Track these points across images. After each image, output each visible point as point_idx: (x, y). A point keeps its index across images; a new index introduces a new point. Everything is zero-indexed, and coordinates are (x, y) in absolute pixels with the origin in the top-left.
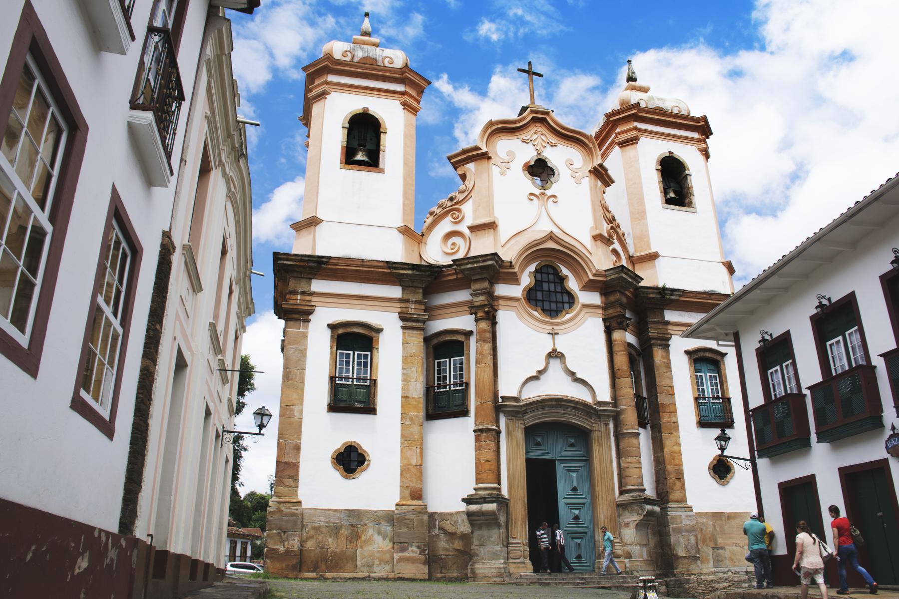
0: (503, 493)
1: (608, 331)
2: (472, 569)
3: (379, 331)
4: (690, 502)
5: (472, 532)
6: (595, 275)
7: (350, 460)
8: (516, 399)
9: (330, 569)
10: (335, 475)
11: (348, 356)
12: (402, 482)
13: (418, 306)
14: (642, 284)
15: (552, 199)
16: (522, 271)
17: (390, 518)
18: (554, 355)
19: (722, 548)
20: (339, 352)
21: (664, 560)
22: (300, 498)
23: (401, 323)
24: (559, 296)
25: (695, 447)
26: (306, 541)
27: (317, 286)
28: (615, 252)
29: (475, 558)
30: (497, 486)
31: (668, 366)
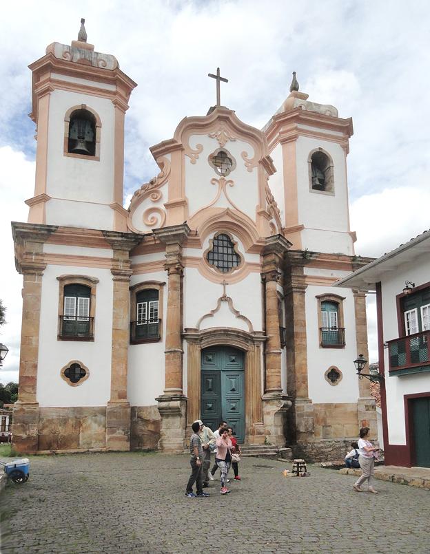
0: (184, 393)
3: (96, 282)
4: (310, 397)
5: (162, 420)
6: (258, 242)
7: (75, 373)
8: (196, 330)
9: (60, 447)
10: (64, 384)
13: (125, 264)
15: (228, 184)
16: (204, 239)
17: (103, 411)
18: (225, 299)
19: (329, 426)
20: (65, 297)
21: (290, 432)
22: (38, 400)
23: (112, 277)
25: (317, 360)
26: (42, 430)
27: (48, 248)
29: (163, 437)
30: (180, 389)
31: (303, 307)
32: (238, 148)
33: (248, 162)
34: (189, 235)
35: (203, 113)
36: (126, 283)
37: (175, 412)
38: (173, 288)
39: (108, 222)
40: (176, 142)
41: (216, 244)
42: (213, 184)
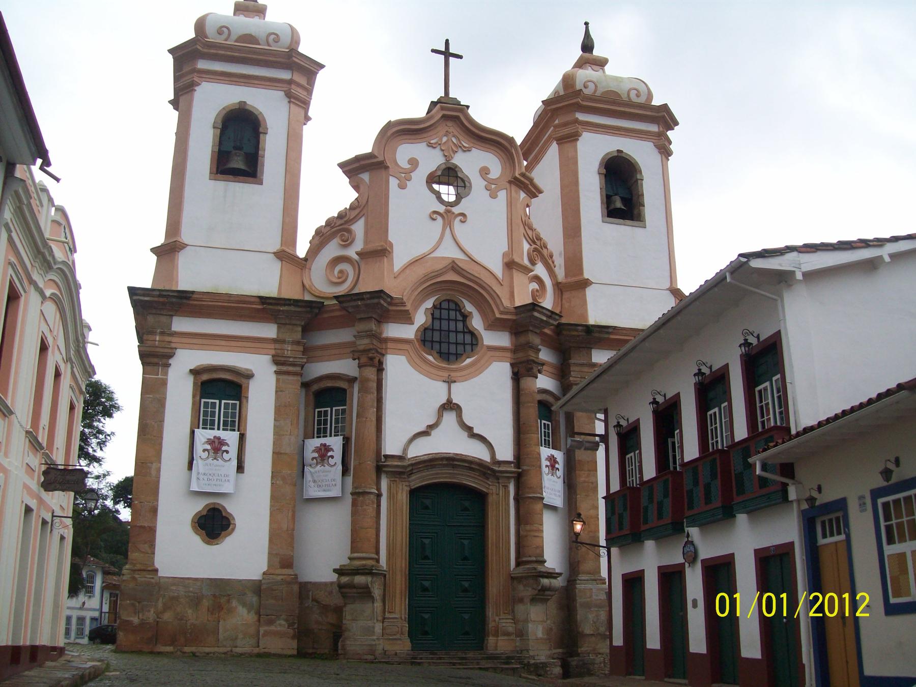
2: (343, 646)
3: (249, 376)
6: (502, 313)
8: (400, 458)
10: (195, 540)
11: (214, 404)
12: (270, 548)
13: (295, 347)
14: (563, 321)
15: (460, 218)
16: (416, 308)
17: (257, 587)
18: (450, 406)
20: (203, 400)
23: (274, 368)
24: (460, 336)
27: (181, 324)
28: (537, 279)
29: (346, 634)
33: (490, 182)
34: (390, 304)
35: (419, 111)
36: (295, 378)
37: (365, 593)
39: (266, 281)
41: (437, 314)
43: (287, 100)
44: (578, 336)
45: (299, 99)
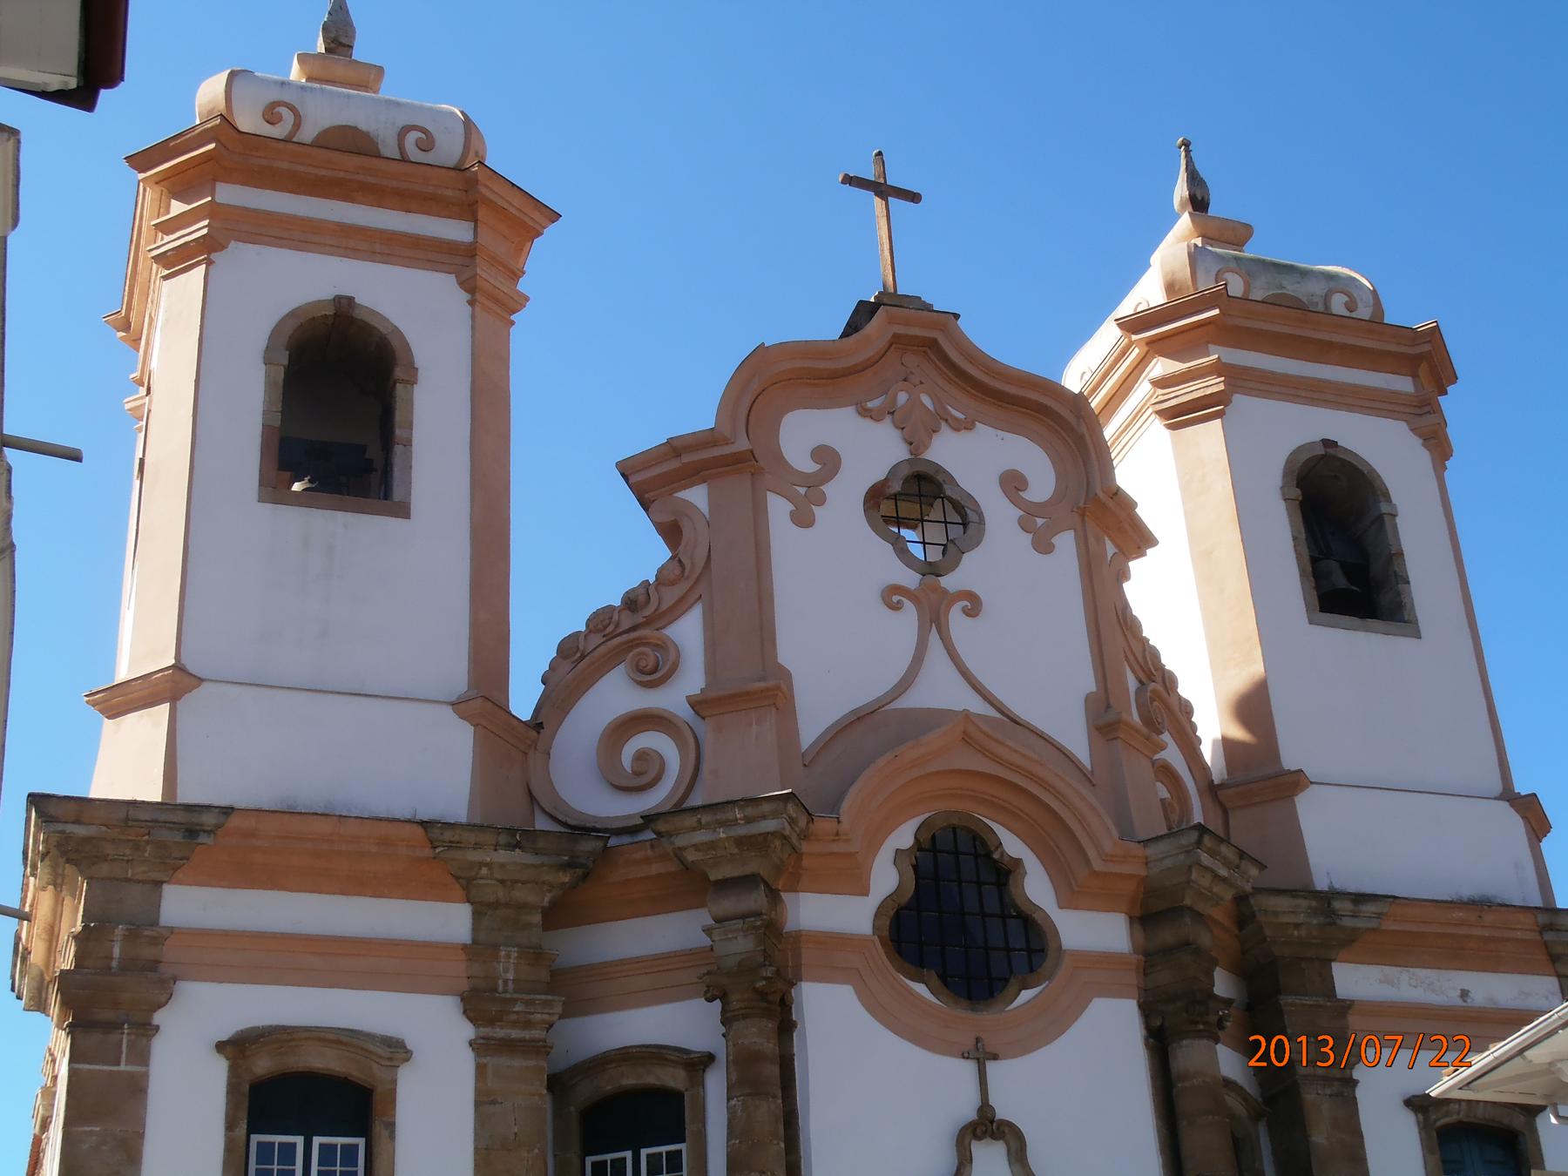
1: (1160, 1042)
11: (288, 1152)
16: (873, 848)
20: (255, 1138)
23: (467, 1031)
27: (186, 905)
32: (975, 457)
38: (744, 1083)
40: (727, 442)
42: (896, 607)
43: (465, 296)
44: (1297, 926)
45: (493, 300)
